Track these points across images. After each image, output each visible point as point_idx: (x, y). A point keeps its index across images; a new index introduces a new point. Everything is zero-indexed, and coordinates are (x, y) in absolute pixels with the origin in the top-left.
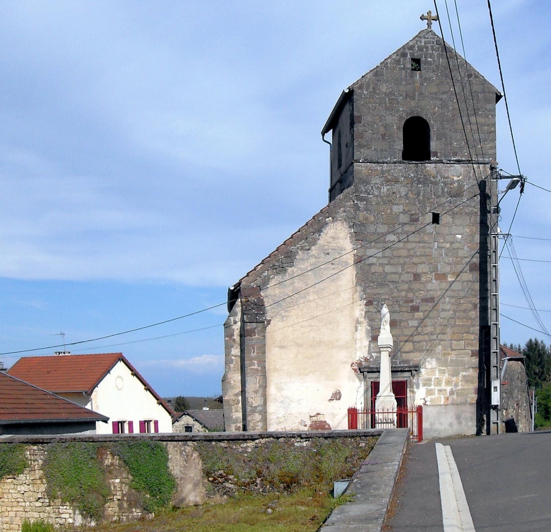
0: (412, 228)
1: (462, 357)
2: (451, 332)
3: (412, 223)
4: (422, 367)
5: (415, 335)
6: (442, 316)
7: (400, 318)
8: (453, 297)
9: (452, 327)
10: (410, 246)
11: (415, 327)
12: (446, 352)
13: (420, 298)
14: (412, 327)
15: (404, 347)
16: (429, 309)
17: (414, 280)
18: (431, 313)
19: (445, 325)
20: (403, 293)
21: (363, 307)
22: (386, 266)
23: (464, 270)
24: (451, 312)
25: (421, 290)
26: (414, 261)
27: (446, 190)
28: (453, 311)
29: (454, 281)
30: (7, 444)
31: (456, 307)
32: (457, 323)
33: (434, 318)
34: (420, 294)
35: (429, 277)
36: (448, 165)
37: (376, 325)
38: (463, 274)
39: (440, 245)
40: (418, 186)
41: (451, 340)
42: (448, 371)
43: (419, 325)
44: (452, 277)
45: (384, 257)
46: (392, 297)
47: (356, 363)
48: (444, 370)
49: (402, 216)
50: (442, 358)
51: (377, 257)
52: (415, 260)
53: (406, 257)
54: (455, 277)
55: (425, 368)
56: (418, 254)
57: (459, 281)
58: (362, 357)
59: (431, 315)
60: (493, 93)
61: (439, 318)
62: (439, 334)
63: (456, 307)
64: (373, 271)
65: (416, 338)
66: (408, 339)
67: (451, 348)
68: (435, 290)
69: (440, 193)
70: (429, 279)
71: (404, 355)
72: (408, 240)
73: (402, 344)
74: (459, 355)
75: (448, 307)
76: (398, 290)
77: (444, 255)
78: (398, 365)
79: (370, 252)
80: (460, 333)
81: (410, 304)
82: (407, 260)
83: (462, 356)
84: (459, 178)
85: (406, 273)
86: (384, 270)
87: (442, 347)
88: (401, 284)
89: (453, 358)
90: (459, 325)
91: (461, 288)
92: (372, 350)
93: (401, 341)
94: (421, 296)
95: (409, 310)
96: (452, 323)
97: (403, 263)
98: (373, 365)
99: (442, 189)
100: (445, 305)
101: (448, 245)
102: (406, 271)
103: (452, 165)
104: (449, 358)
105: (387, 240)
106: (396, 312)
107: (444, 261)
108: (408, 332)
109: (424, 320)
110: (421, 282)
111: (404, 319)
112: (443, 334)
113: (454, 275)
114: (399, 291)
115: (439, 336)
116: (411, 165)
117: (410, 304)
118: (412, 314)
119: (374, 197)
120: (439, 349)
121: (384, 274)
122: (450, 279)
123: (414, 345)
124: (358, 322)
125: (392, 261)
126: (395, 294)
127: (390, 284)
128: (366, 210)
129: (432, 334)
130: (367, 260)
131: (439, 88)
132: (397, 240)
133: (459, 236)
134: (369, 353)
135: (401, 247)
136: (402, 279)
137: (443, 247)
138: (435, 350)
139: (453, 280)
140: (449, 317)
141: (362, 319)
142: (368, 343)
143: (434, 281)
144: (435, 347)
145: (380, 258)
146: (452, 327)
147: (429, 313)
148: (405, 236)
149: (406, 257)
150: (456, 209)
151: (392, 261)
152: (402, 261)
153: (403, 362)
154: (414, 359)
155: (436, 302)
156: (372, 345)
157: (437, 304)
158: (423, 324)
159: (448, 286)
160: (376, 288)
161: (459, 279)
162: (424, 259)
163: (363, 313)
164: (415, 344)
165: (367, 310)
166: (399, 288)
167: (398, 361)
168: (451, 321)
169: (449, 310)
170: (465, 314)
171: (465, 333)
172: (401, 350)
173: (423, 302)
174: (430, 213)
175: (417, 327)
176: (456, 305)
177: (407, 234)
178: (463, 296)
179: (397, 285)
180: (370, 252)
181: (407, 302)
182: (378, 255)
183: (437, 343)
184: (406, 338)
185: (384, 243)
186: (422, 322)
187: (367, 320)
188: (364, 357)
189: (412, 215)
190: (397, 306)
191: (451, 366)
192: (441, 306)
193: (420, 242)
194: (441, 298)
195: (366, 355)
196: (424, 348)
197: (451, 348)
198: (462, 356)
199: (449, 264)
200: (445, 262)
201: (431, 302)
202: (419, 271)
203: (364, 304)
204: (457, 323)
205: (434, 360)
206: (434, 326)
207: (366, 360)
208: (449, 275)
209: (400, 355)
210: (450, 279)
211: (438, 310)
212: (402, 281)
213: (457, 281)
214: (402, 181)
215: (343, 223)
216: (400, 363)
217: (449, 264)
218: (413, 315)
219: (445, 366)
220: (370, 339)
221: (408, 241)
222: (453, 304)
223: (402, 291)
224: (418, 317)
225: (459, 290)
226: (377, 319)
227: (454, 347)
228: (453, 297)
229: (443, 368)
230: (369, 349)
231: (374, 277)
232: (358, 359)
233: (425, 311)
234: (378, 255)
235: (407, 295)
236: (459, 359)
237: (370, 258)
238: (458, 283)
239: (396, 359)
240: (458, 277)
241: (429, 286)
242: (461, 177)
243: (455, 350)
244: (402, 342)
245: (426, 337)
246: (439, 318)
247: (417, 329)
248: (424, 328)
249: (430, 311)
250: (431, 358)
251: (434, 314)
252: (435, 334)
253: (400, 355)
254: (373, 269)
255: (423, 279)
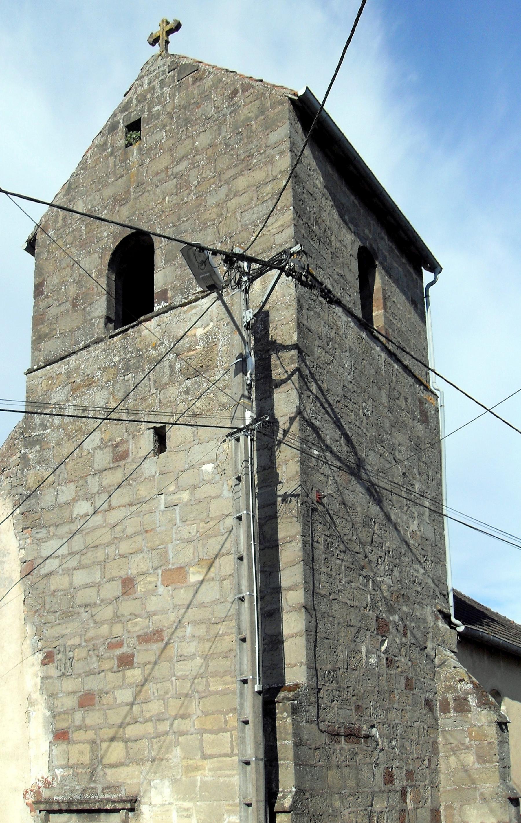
0: (117, 477)
1: (228, 776)
2: (199, 713)
3: (116, 464)
4: (143, 800)
5: (129, 724)
6: (179, 674)
7: (99, 688)
8: (201, 622)
9: (200, 698)
10: (114, 517)
11: (127, 705)
12: (191, 762)
13: (135, 635)
14: (122, 704)
15: (109, 754)
16: (153, 659)
17: (123, 594)
18: (157, 667)
19: (186, 696)
20: (105, 629)
21: (38, 668)
22: (75, 572)
23: (223, 551)
24: (199, 661)
25: (137, 616)
26: (122, 551)
27: (178, 366)
28: (201, 657)
29: (202, 582)
30: (194, 735)
31: (207, 645)
32: (211, 688)
33: (164, 680)
34: (136, 624)
35: (150, 583)
36: (185, 308)
37: (59, 705)
38: (222, 558)
39: (169, 498)
40: (126, 378)
41: (202, 731)
42: (198, 812)
43: (135, 699)
44: (199, 572)
45: (72, 554)
46: (86, 641)
47: (32, 791)
48: (188, 810)
49: (99, 454)
50: (184, 779)
51: (58, 557)
52: (124, 547)
53: (109, 544)
54: (204, 571)
55: (150, 804)
56: (130, 531)
57: (213, 579)
58: (40, 778)
59: (156, 673)
60: (281, 103)
61: (174, 679)
62: (175, 718)
63: (207, 645)
64: (53, 588)
65: (131, 731)
66: (116, 733)
67: (203, 752)
68: (165, 611)
69: (166, 379)
70: (150, 587)
71: (109, 771)
72: (110, 505)
73: (105, 745)
74: (220, 769)
75: (191, 648)
76: (95, 622)
77: (178, 521)
78: (101, 797)
79: (47, 549)
80: (220, 712)
81: (118, 652)
82: (111, 551)
83: (228, 772)
84: (207, 329)
85: (109, 581)
86: (71, 584)
87: (182, 749)
88: (100, 608)
89: (206, 779)
90: (216, 693)
91: (218, 597)
92: (56, 763)
93: (103, 741)
94: (137, 628)
95: (116, 666)
96: (201, 688)
97: (102, 559)
98: (58, 796)
99: (171, 366)
100: (184, 644)
101: (185, 496)
102: (108, 576)
103: (194, 304)
104: (199, 778)
105: (74, 516)
106: (95, 674)
107: (179, 536)
108: (115, 718)
109: (143, 685)
110: (136, 595)
111: (106, 689)
112: (184, 717)
113: (201, 567)
114: (98, 624)
115: (176, 722)
116: (115, 339)
117: (118, 652)
118: (120, 674)
119: (53, 431)
120: (176, 757)
121: (72, 590)
122: (194, 577)
123: (127, 747)
124: (30, 702)
125: (85, 561)
126: (91, 633)
127: (82, 610)
128: (39, 462)
129: (160, 719)
130: (41, 566)
131: (172, 156)
132: (91, 511)
133: (209, 468)
134: (51, 769)
135: (98, 524)
136: (101, 597)
137: (176, 502)
138: (167, 760)
139: (201, 578)
140: (194, 673)
141: (37, 696)
142: (47, 746)
143: (161, 589)
144: (167, 753)
145: (63, 557)
146: (200, 698)
147: (153, 668)
148: (104, 496)
149: (109, 544)
150: (199, 404)
151: (85, 561)
152: (100, 555)
153: (106, 789)
154: (129, 782)
155: (166, 639)
156: (55, 752)
157: (167, 644)
158: (142, 696)
159: (191, 595)
160: (59, 624)
161: (211, 574)
162: (140, 541)
163: (39, 680)
164: (130, 744)
165: (45, 674)
166: (97, 618)
167: (99, 787)
168: (199, 684)
169: (193, 657)
170: (229, 663)
171: (231, 712)
172: (105, 761)
173: (140, 643)
174: (148, 431)
175: (132, 704)
176: (207, 640)
177: (109, 492)
178: (223, 615)
179: (95, 611)
180: (47, 549)
181: (111, 647)
182: (60, 552)
183: (171, 742)
184: (110, 733)
185: (70, 523)
186: (140, 691)
187: (45, 697)
188: (43, 777)
189: (117, 446)
190: (94, 659)
191: (202, 799)
192: (174, 650)
193: (131, 504)
194: (176, 628)
195: (46, 774)
196: (146, 753)
197: (203, 752)
198: (228, 772)
199: (190, 541)
200: (181, 539)
201: (157, 641)
202: (132, 571)
203: (40, 661)
204: (211, 688)
205: (167, 783)
206: (164, 700)
207: (48, 784)
208: (192, 570)
209: (101, 773)
210: (194, 577)
211: (170, 660)
212: (102, 601)
213: (208, 581)
214: (98, 380)
215: (5, 499)
216: (103, 792)
217: (190, 541)
218: (124, 676)
219: (191, 800)
220: (51, 737)
221: (110, 508)
222: (201, 639)
223: (102, 623)
224: (132, 680)
225: (215, 602)
226: (61, 691)
227: (208, 751)
228: (201, 622)
229: (187, 804)
230: (50, 761)
231: (55, 601)
232: (33, 781)
233: (146, 664)
234: (60, 552)
235: (111, 631)
236: (222, 780)
237: (47, 561)
238: (212, 583)
239: (95, 782)
240: (209, 569)
241: (153, 603)
242: (212, 324)
243: (211, 757)
244: (105, 741)
245: (149, 727)
246: (174, 679)
247: (131, 708)
248: (145, 706)
249: (155, 663)
250: (161, 780)
251: (163, 668)
252: (167, 719)
253: (101, 773)
254: (55, 583)
255: (140, 588)
